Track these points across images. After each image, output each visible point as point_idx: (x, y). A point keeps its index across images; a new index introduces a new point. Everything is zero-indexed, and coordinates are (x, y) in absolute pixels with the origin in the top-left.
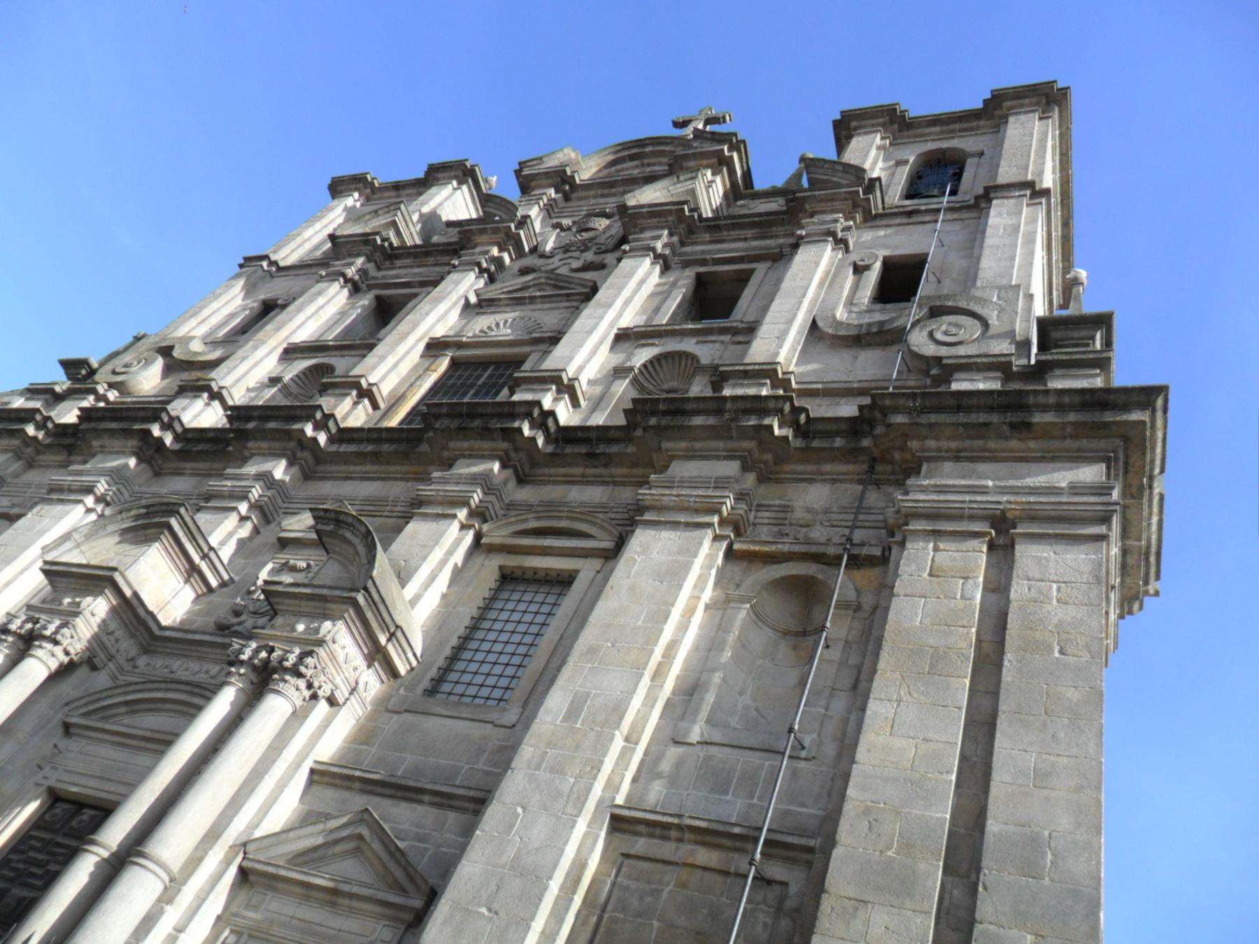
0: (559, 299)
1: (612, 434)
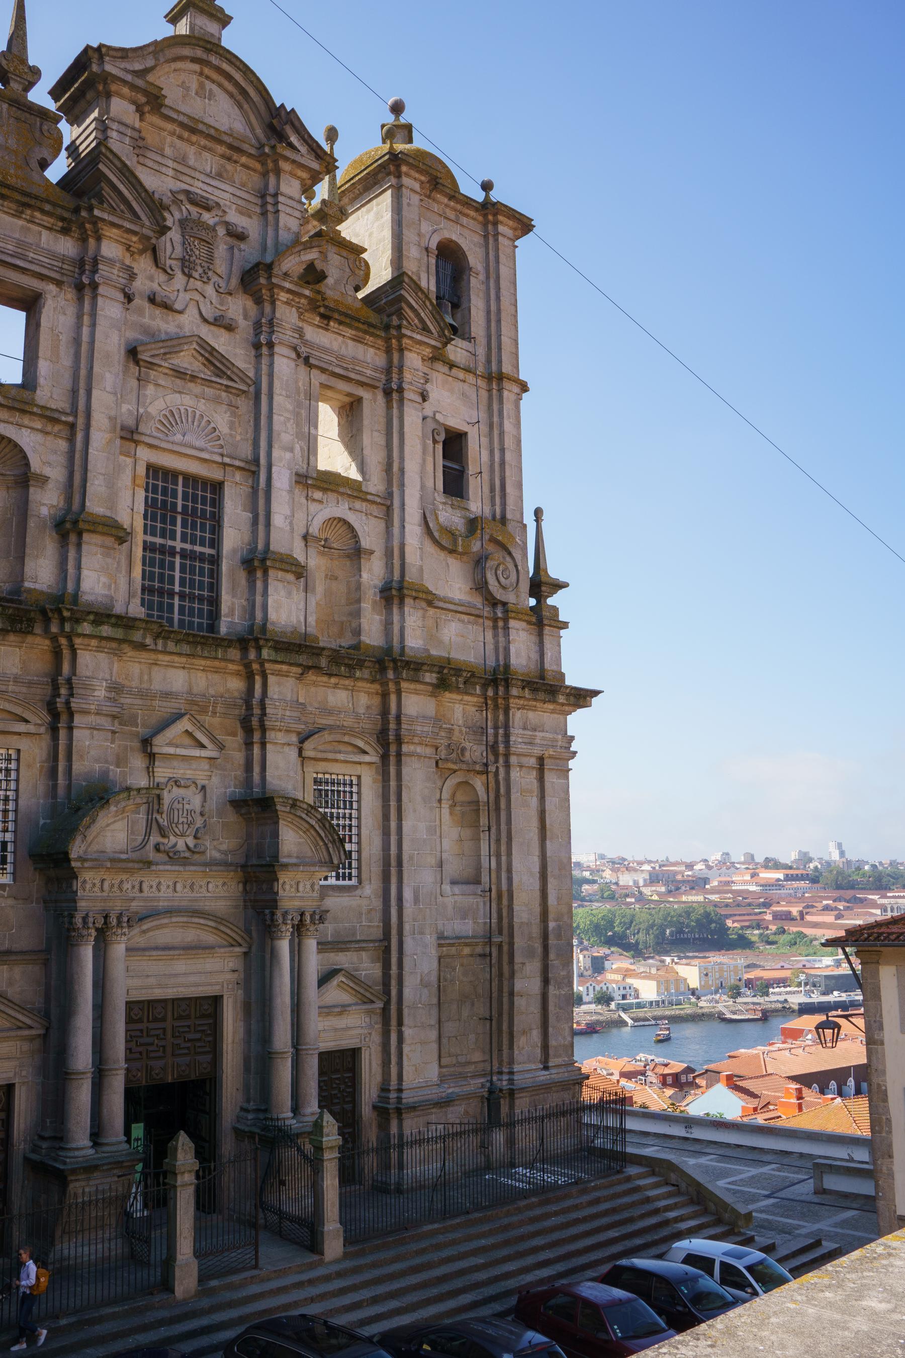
0: (219, 386)
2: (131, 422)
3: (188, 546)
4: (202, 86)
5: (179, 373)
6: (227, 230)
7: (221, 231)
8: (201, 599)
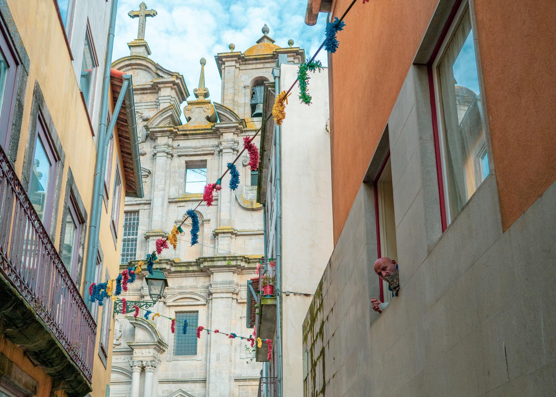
1: (193, 264)
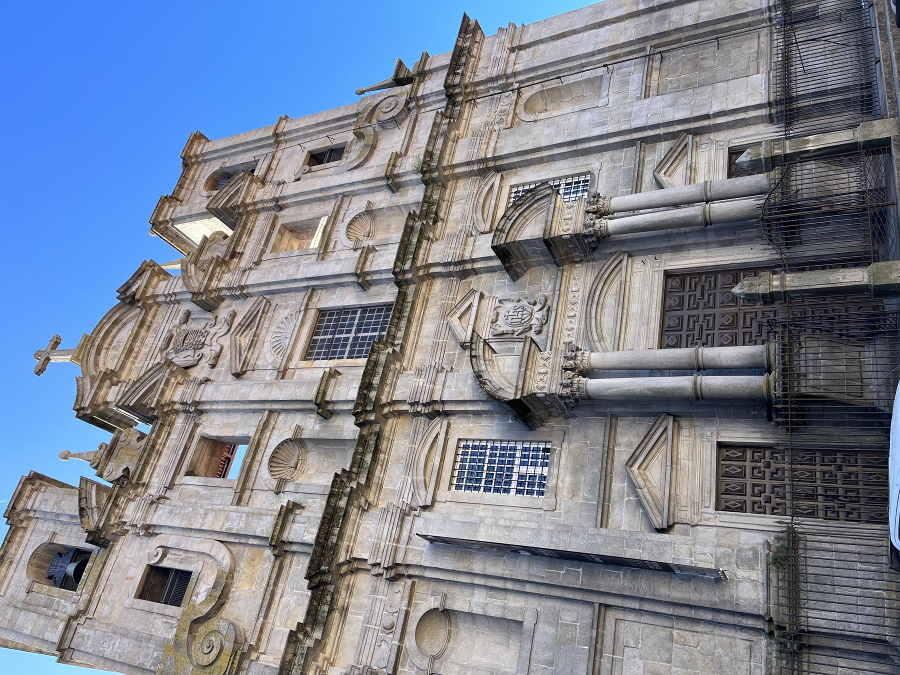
0: (263, 318)
2: (276, 373)
3: (354, 328)
4: (114, 348)
5: (252, 344)
6: (183, 323)
7: (184, 327)
8: (387, 316)
